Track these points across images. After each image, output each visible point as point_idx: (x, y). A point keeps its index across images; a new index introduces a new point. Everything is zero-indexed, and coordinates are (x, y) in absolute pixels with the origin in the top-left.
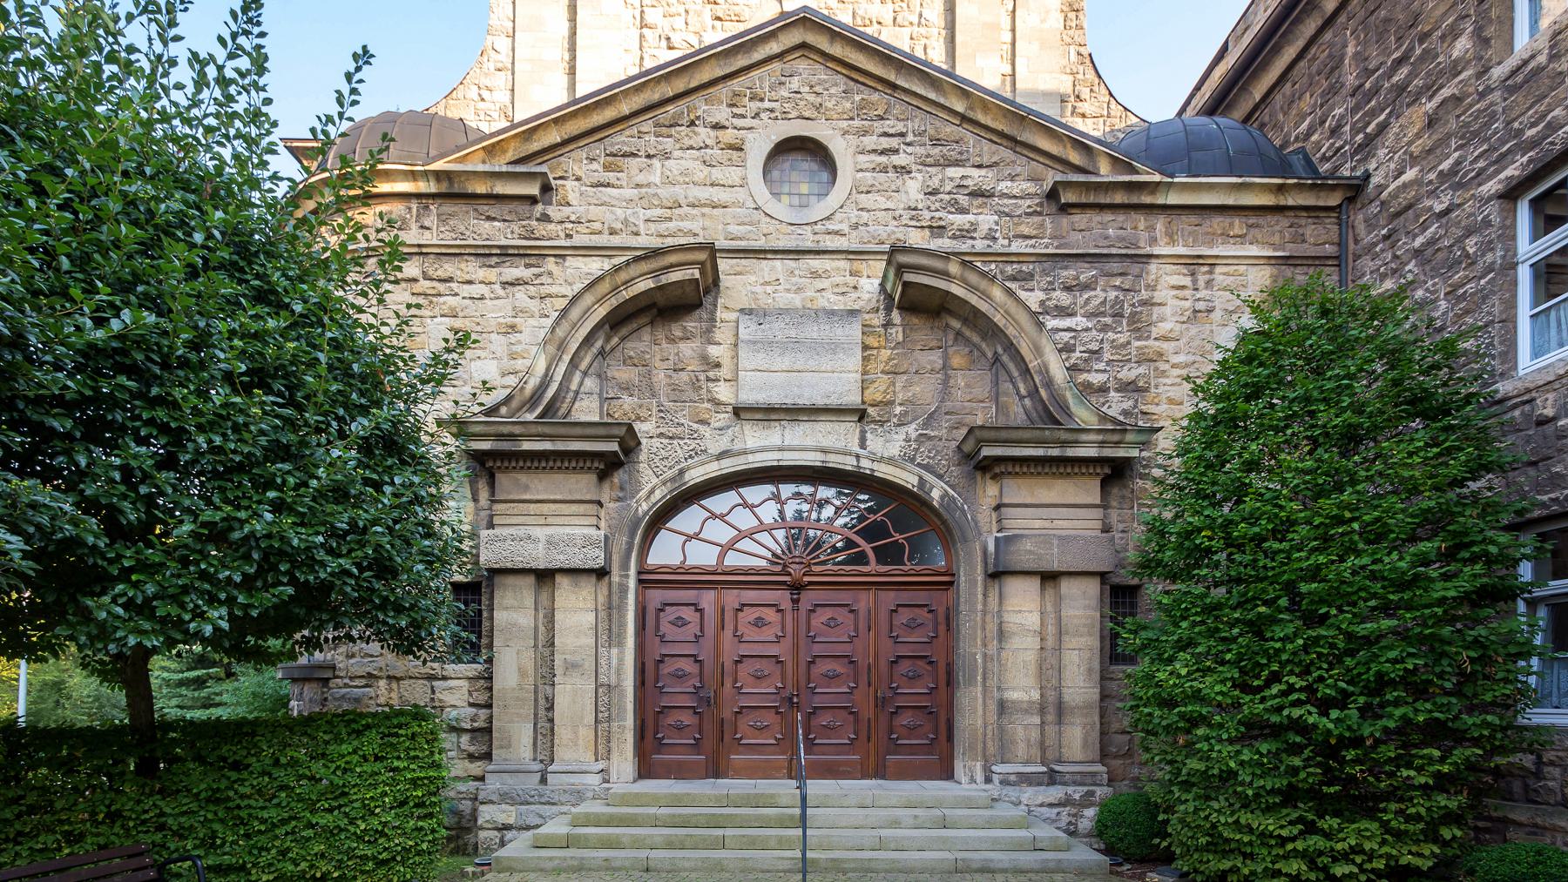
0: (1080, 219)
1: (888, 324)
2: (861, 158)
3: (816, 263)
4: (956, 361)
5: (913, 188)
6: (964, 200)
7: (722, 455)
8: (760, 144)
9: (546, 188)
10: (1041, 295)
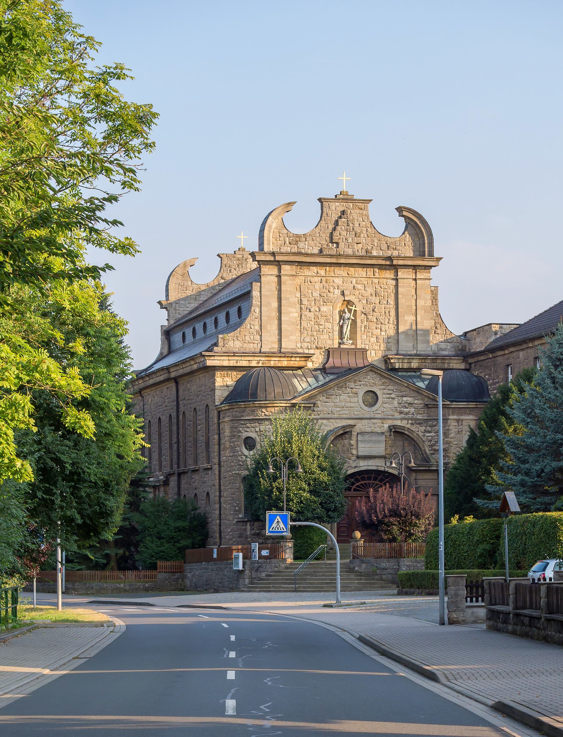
0: (432, 409)
1: (390, 435)
2: (384, 395)
3: (374, 421)
4: (406, 445)
5: (396, 402)
6: (407, 405)
7: (356, 467)
8: (361, 393)
9: (314, 404)
10: (424, 428)
